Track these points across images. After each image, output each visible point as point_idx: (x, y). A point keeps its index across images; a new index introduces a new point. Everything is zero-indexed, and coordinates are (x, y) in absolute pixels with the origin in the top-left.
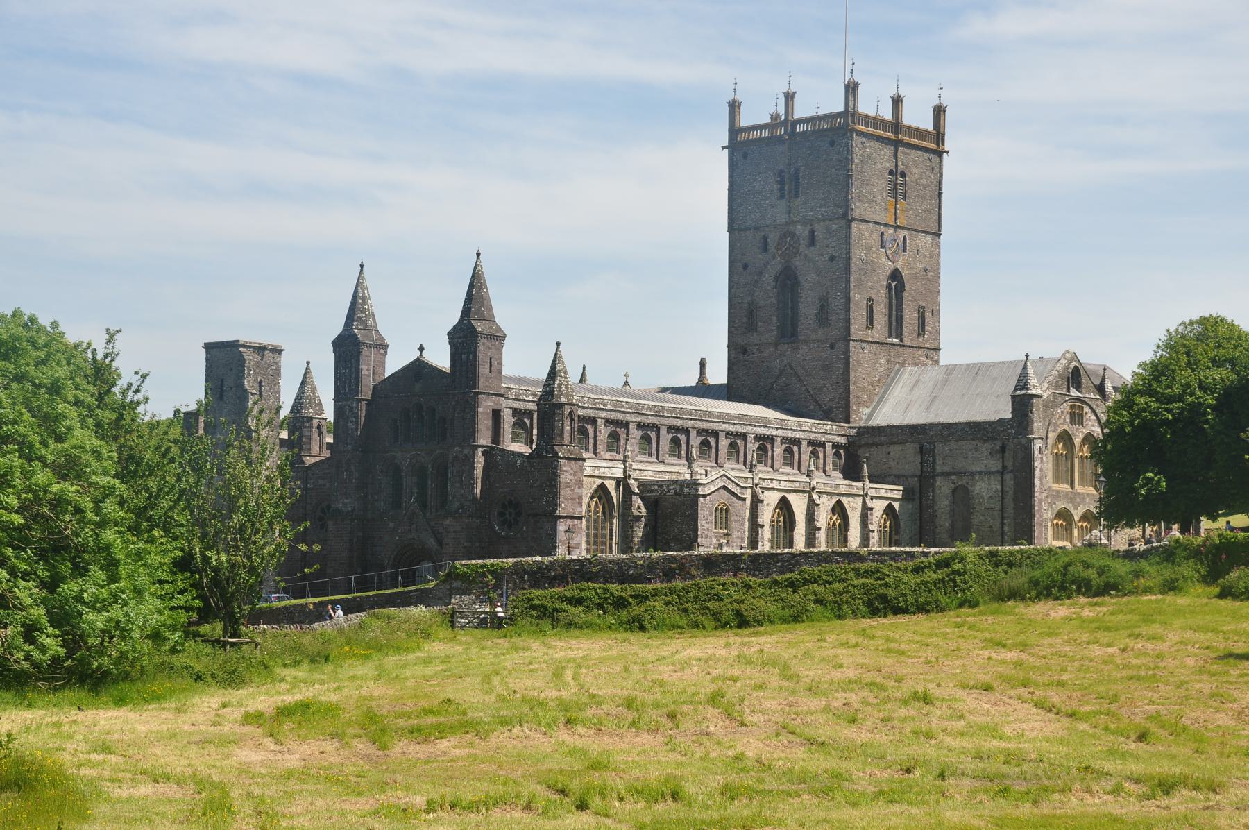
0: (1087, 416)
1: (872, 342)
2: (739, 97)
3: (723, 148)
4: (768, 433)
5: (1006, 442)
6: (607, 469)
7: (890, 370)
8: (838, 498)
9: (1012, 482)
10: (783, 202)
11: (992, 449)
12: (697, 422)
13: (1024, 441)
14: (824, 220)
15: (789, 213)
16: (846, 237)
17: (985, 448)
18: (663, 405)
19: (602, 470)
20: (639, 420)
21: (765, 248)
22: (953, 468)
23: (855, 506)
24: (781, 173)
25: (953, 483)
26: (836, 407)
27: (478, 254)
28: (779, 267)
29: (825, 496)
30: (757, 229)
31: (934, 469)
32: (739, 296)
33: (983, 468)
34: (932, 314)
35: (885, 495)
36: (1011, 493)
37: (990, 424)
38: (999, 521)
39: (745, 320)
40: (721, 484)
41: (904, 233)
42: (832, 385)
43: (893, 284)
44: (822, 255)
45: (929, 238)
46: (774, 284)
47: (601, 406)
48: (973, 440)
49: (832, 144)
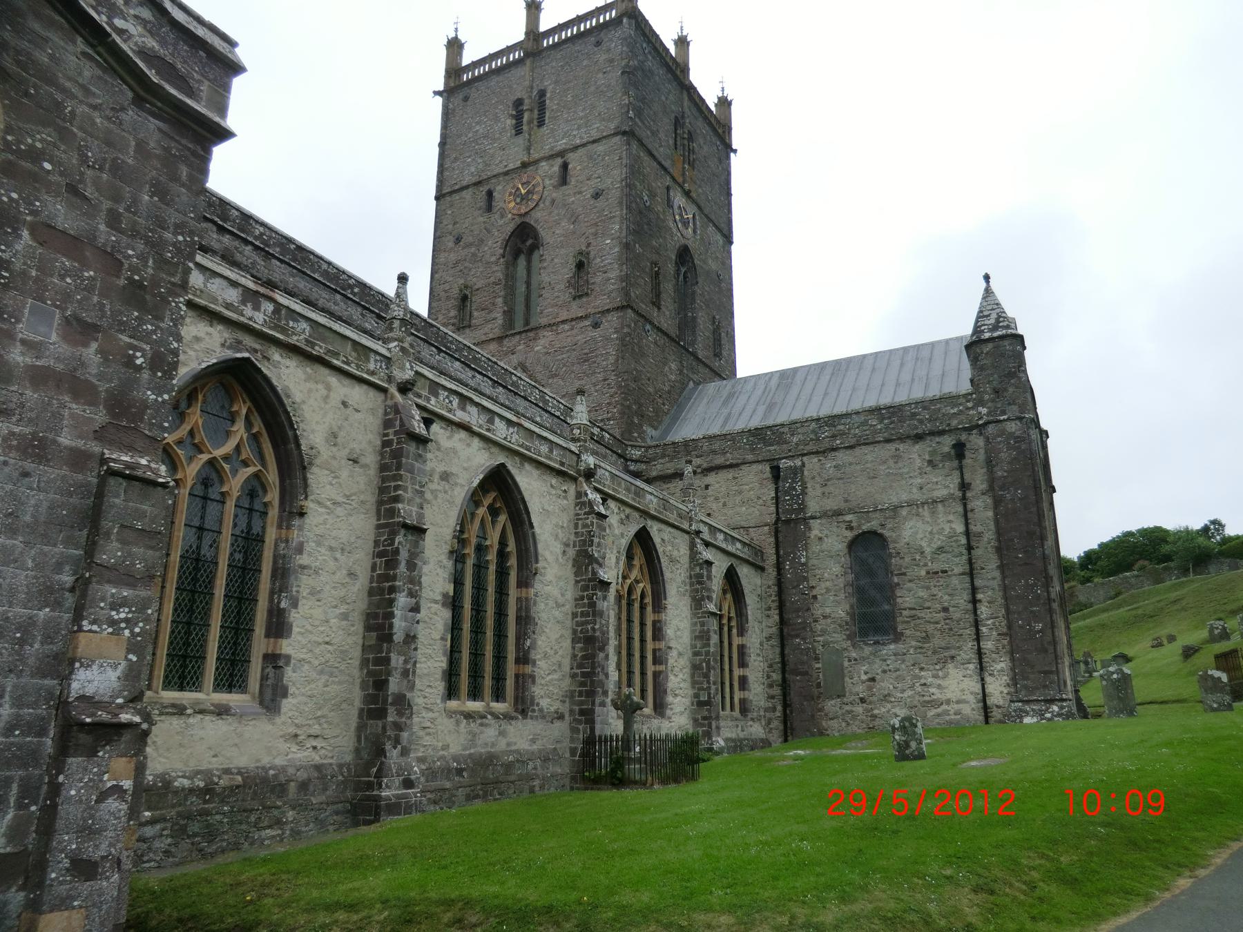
2: (462, 37)
3: (436, 93)
5: (964, 437)
7: (684, 386)
9: (990, 514)
10: (521, 140)
11: (933, 453)
13: (1012, 427)
14: (583, 145)
15: (528, 149)
16: (620, 158)
17: (916, 454)
21: (489, 208)
22: (846, 501)
24: (518, 103)
25: (851, 528)
26: (602, 420)
28: (510, 228)
30: (478, 184)
31: (802, 508)
32: (446, 282)
33: (916, 495)
35: (724, 546)
36: (989, 535)
37: (924, 404)
38: (966, 596)
39: (453, 313)
42: (594, 384)
43: (683, 270)
44: (580, 193)
46: (502, 251)
48: (888, 441)
49: (598, 44)
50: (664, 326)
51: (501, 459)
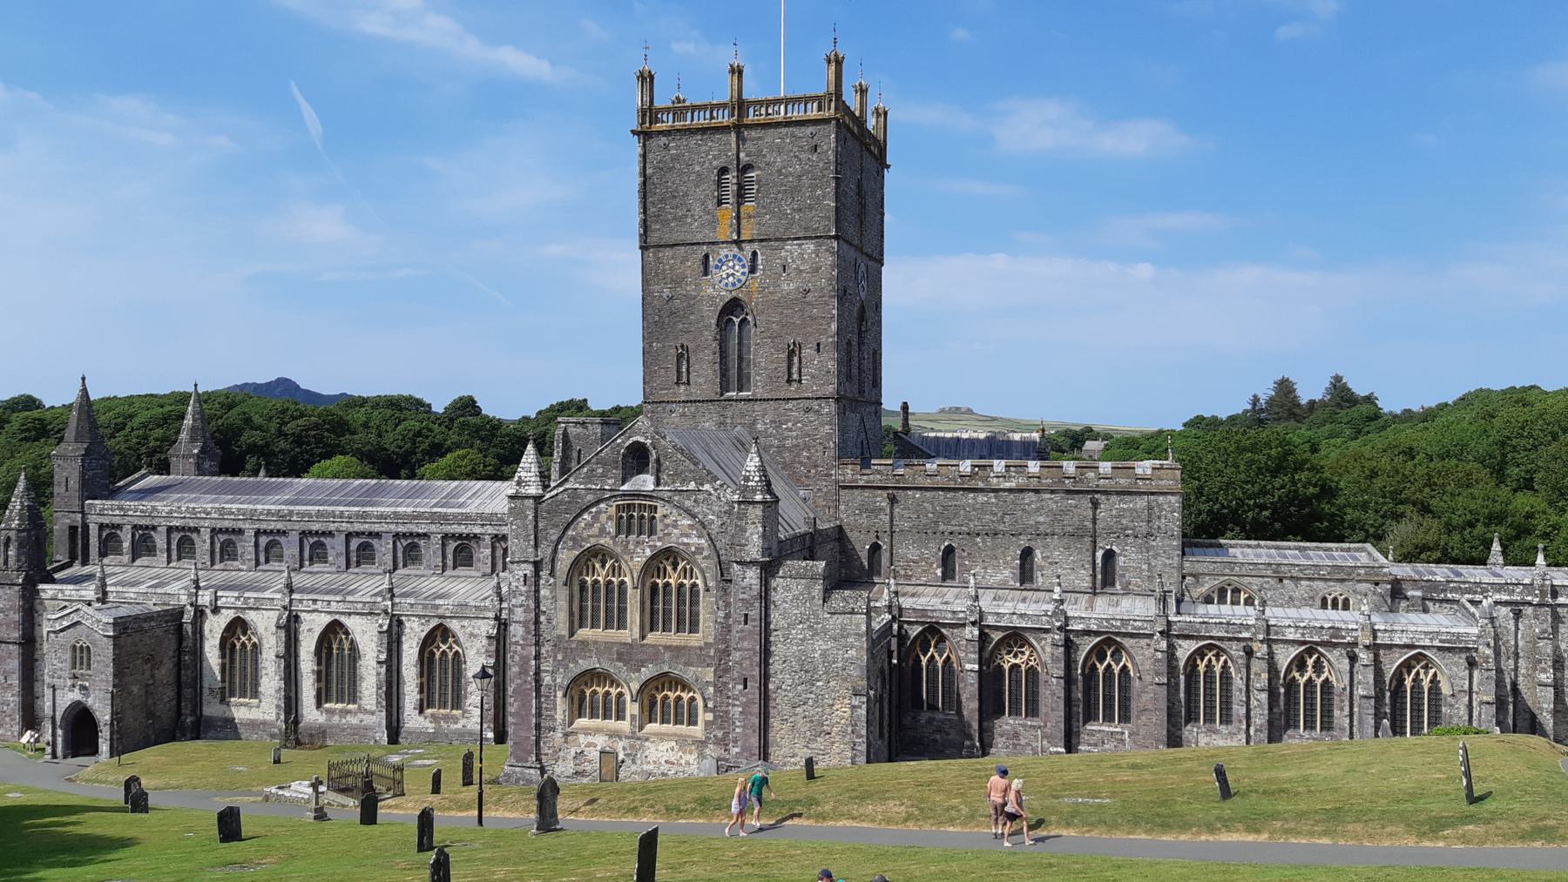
0: (668, 521)
1: (687, 402)
4: (466, 531)
6: (73, 592)
8: (440, 621)
12: (344, 524)
18: (292, 508)
19: (67, 593)
20: (256, 526)
23: (476, 632)
27: (83, 379)
29: (413, 618)
34: (818, 350)
40: (75, 620)
41: (756, 246)
45: (810, 246)
47: (203, 515)
50: (696, 392)
51: (337, 617)
